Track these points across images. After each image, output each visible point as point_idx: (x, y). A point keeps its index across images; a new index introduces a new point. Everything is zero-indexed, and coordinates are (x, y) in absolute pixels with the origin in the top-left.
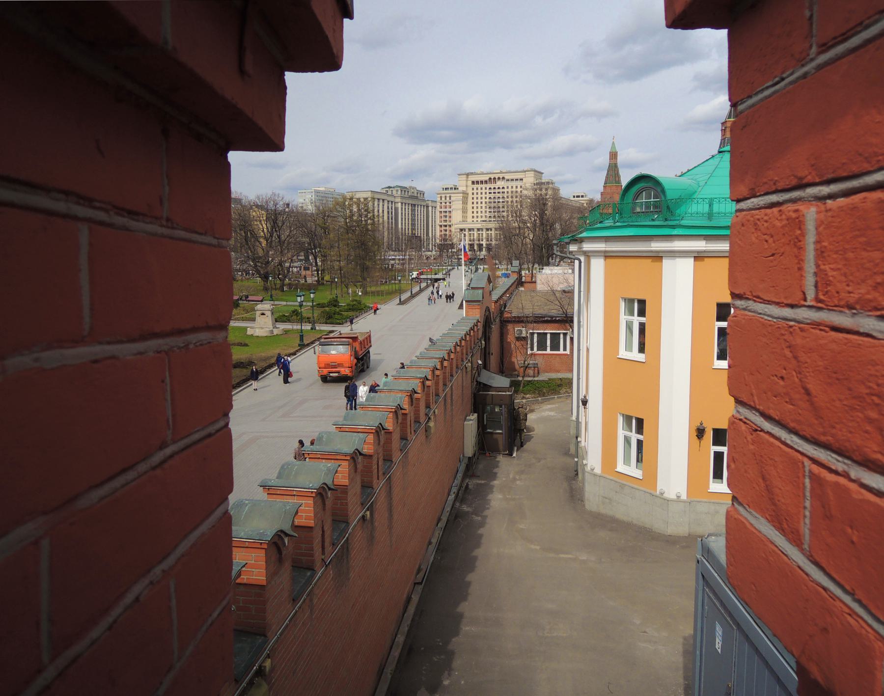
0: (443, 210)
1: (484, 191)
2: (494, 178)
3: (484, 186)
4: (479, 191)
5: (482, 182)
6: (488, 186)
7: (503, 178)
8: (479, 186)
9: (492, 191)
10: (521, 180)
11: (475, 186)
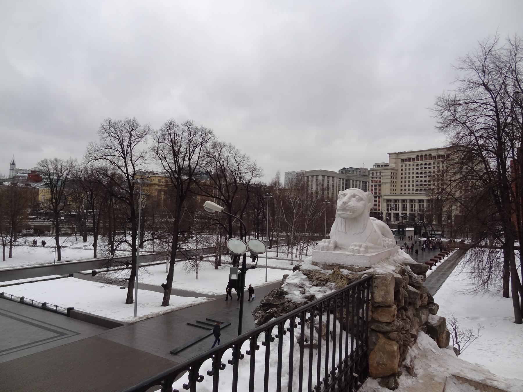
0: (374, 183)
1: (411, 167)
2: (422, 156)
3: (412, 163)
4: (408, 167)
6: (416, 163)
7: (430, 155)
8: (408, 163)
9: (419, 167)
11: (404, 164)
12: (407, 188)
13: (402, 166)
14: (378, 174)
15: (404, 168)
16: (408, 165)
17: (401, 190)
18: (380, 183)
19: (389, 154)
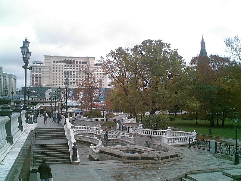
0: (35, 76)
3: (61, 64)
4: (58, 67)
5: (60, 62)
10: (86, 63)
12: (58, 81)
13: (54, 65)
14: (38, 70)
15: (55, 67)
16: (58, 65)
17: (54, 82)
18: (40, 77)
19: (44, 56)
